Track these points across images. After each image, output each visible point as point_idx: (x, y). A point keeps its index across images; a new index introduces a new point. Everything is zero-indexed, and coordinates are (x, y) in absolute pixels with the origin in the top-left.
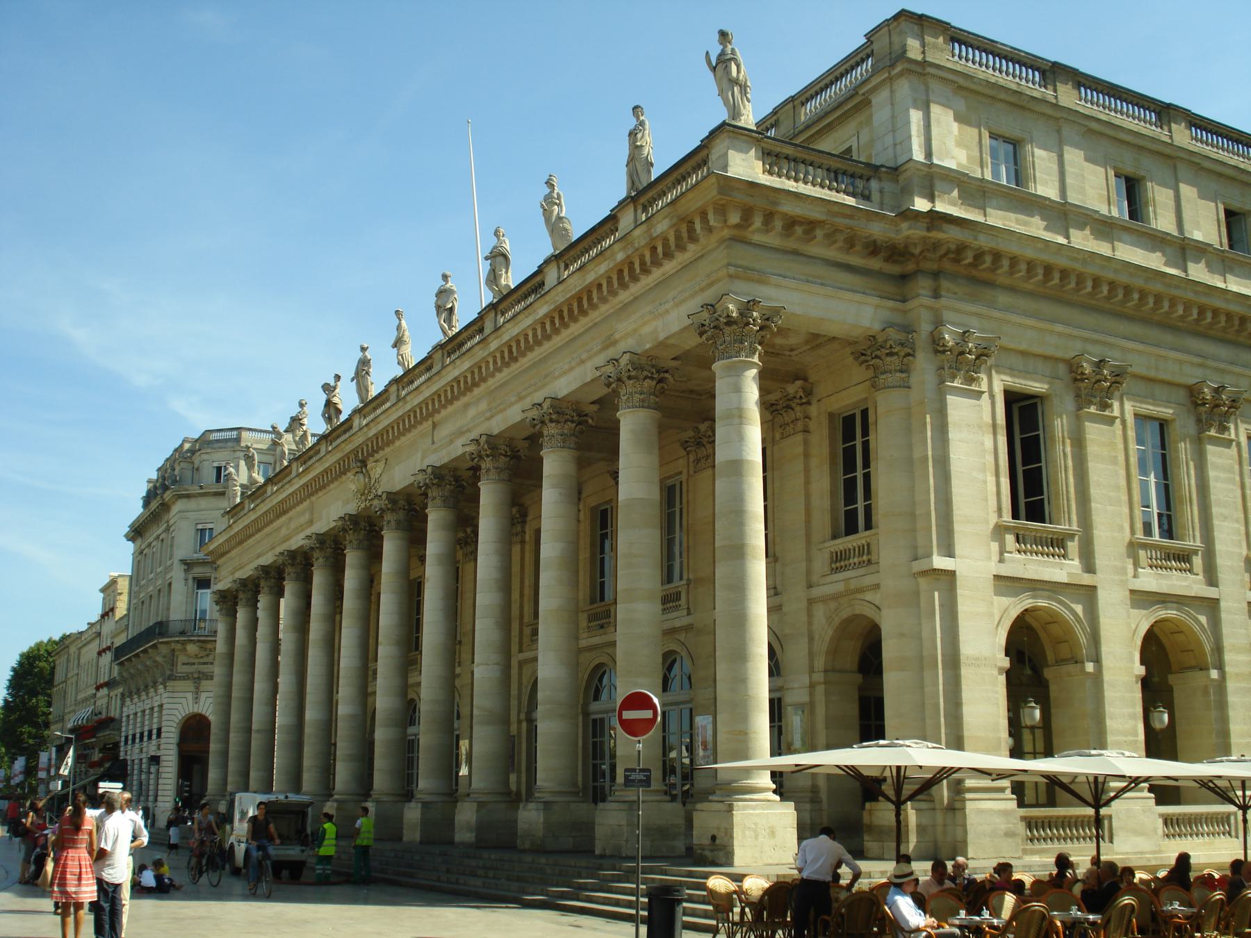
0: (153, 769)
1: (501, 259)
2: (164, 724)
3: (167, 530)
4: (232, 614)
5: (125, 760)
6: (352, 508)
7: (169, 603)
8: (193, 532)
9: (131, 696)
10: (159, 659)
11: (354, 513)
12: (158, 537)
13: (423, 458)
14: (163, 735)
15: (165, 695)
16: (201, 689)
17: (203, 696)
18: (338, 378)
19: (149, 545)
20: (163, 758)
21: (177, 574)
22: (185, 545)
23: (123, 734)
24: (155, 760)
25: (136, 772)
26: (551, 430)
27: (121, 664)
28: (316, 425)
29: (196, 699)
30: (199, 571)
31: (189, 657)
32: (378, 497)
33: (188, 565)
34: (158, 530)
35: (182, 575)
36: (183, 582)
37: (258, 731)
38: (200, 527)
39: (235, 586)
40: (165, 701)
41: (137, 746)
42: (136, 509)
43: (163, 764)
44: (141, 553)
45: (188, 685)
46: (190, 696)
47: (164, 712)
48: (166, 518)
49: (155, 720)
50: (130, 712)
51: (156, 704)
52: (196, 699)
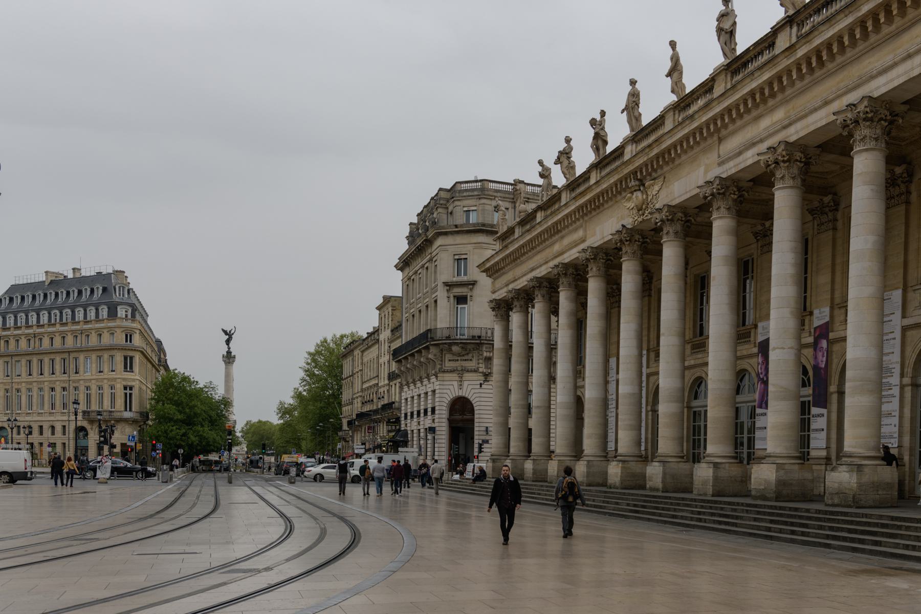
0: (430, 437)
2: (437, 404)
3: (431, 260)
4: (506, 319)
5: (406, 431)
6: (629, 222)
7: (436, 315)
8: (452, 261)
9: (408, 384)
10: (430, 356)
11: (629, 226)
12: (423, 266)
13: (706, 172)
14: (437, 412)
15: (438, 383)
16: (464, 378)
17: (466, 384)
19: (416, 273)
20: (437, 429)
21: (441, 293)
22: (446, 271)
23: (403, 412)
24: (432, 430)
25: (415, 439)
26: (863, 131)
27: (399, 361)
28: (584, 158)
29: (461, 386)
31: (454, 354)
32: (659, 210)
33: (449, 285)
35: (446, 294)
36: (446, 300)
38: (457, 257)
39: (510, 295)
40: (437, 387)
41: (415, 420)
42: (403, 246)
43: (437, 433)
44: (409, 279)
45: (454, 376)
46: (455, 384)
47: (437, 396)
48: (429, 251)
49: (429, 401)
50: (408, 397)
51: (429, 390)
52: (461, 386)
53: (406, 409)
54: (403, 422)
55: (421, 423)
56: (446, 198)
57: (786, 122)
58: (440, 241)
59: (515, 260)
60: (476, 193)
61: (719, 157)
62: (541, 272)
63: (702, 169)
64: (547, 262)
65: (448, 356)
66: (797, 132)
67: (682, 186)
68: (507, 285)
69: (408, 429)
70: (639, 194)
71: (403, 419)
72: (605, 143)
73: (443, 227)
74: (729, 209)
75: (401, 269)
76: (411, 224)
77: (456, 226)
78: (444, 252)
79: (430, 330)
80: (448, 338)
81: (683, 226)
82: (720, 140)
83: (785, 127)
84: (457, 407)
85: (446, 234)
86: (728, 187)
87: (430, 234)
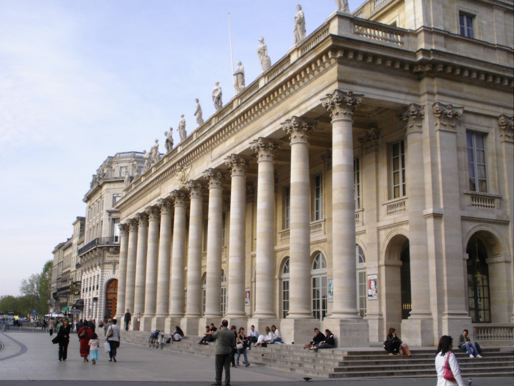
0: (95, 304)
1: (240, 75)
3: (101, 197)
9: (85, 271)
11: (178, 189)
12: (97, 201)
13: (207, 164)
18: (172, 129)
19: (93, 204)
21: (105, 217)
23: (82, 288)
24: (95, 299)
25: (87, 305)
27: (81, 257)
29: (114, 272)
30: (114, 215)
31: (111, 253)
32: (188, 182)
33: (110, 213)
34: (97, 197)
35: (108, 217)
36: (108, 220)
37: (138, 286)
42: (87, 189)
44: (90, 207)
46: (111, 271)
48: (100, 192)
52: (114, 272)
53: (84, 286)
54: (82, 294)
55: (91, 295)
56: (110, 162)
57: (235, 145)
58: (105, 187)
59: (130, 203)
60: (128, 159)
61: (211, 157)
62: (141, 211)
63: (206, 163)
64: (144, 205)
65: (107, 254)
66: (239, 149)
67: (198, 170)
68: (127, 216)
69: (84, 298)
70: (180, 173)
71: (82, 292)
72: (172, 144)
73: (108, 179)
74: (217, 183)
75: (86, 202)
76: (94, 176)
77: (115, 178)
78: (108, 193)
79: (98, 239)
80: (108, 243)
81: (201, 190)
82: (212, 149)
83: (235, 147)
84: (111, 285)
85: (110, 182)
86: (216, 173)
87: (101, 183)
